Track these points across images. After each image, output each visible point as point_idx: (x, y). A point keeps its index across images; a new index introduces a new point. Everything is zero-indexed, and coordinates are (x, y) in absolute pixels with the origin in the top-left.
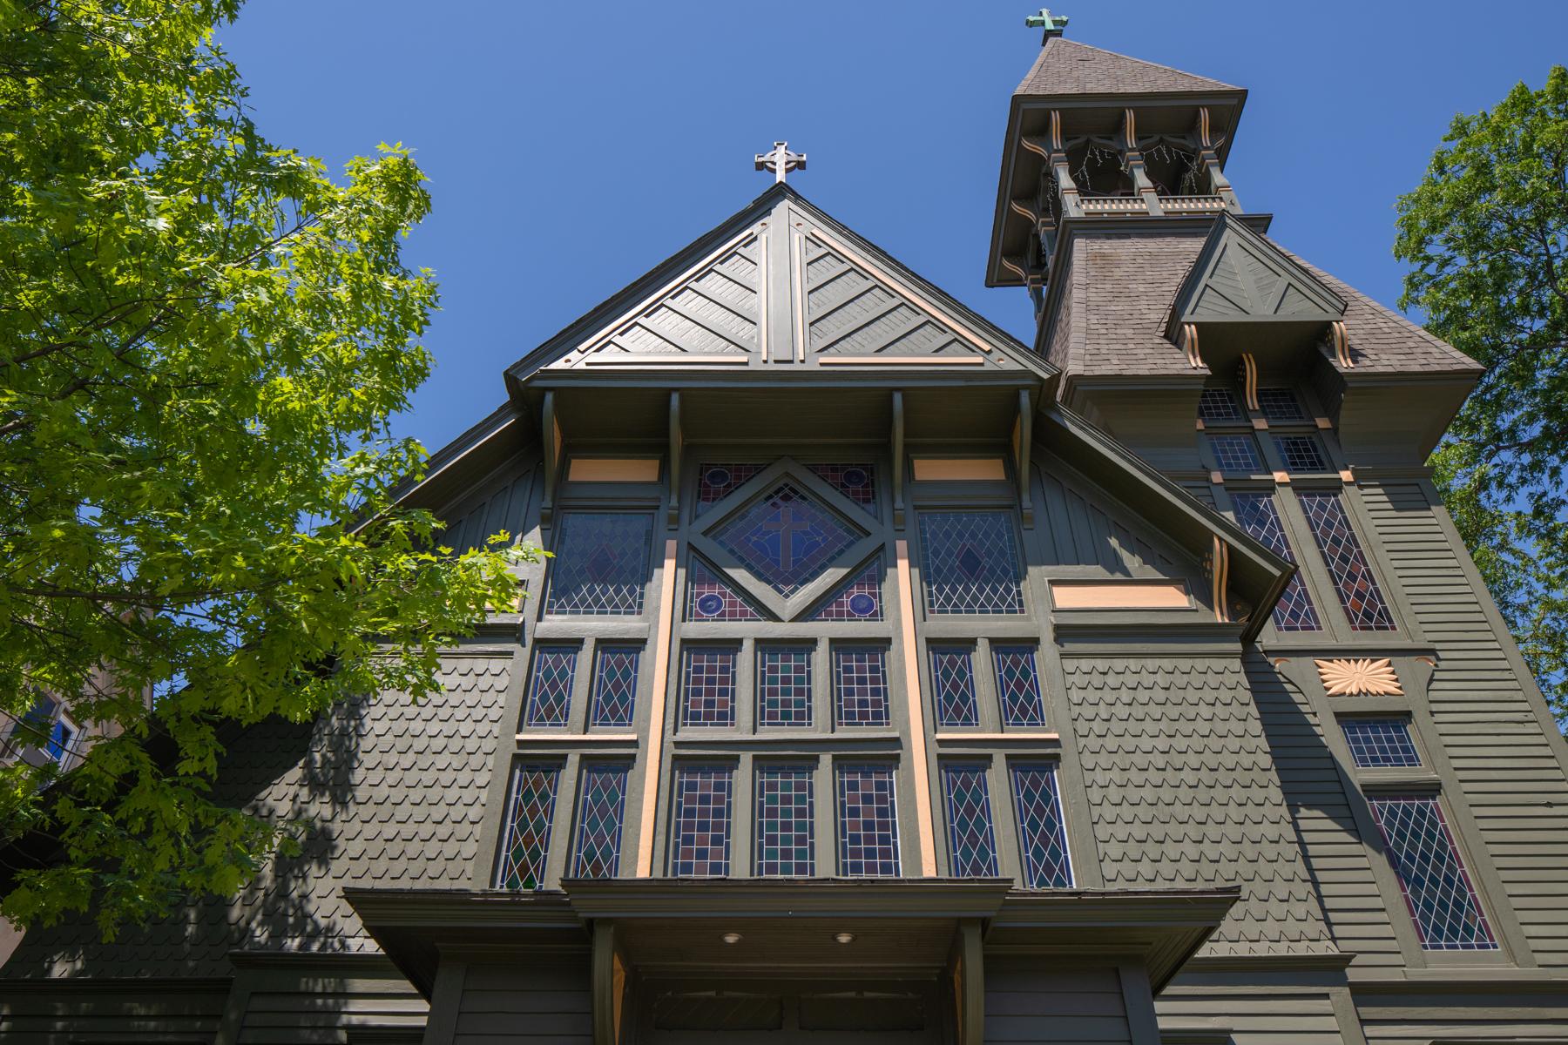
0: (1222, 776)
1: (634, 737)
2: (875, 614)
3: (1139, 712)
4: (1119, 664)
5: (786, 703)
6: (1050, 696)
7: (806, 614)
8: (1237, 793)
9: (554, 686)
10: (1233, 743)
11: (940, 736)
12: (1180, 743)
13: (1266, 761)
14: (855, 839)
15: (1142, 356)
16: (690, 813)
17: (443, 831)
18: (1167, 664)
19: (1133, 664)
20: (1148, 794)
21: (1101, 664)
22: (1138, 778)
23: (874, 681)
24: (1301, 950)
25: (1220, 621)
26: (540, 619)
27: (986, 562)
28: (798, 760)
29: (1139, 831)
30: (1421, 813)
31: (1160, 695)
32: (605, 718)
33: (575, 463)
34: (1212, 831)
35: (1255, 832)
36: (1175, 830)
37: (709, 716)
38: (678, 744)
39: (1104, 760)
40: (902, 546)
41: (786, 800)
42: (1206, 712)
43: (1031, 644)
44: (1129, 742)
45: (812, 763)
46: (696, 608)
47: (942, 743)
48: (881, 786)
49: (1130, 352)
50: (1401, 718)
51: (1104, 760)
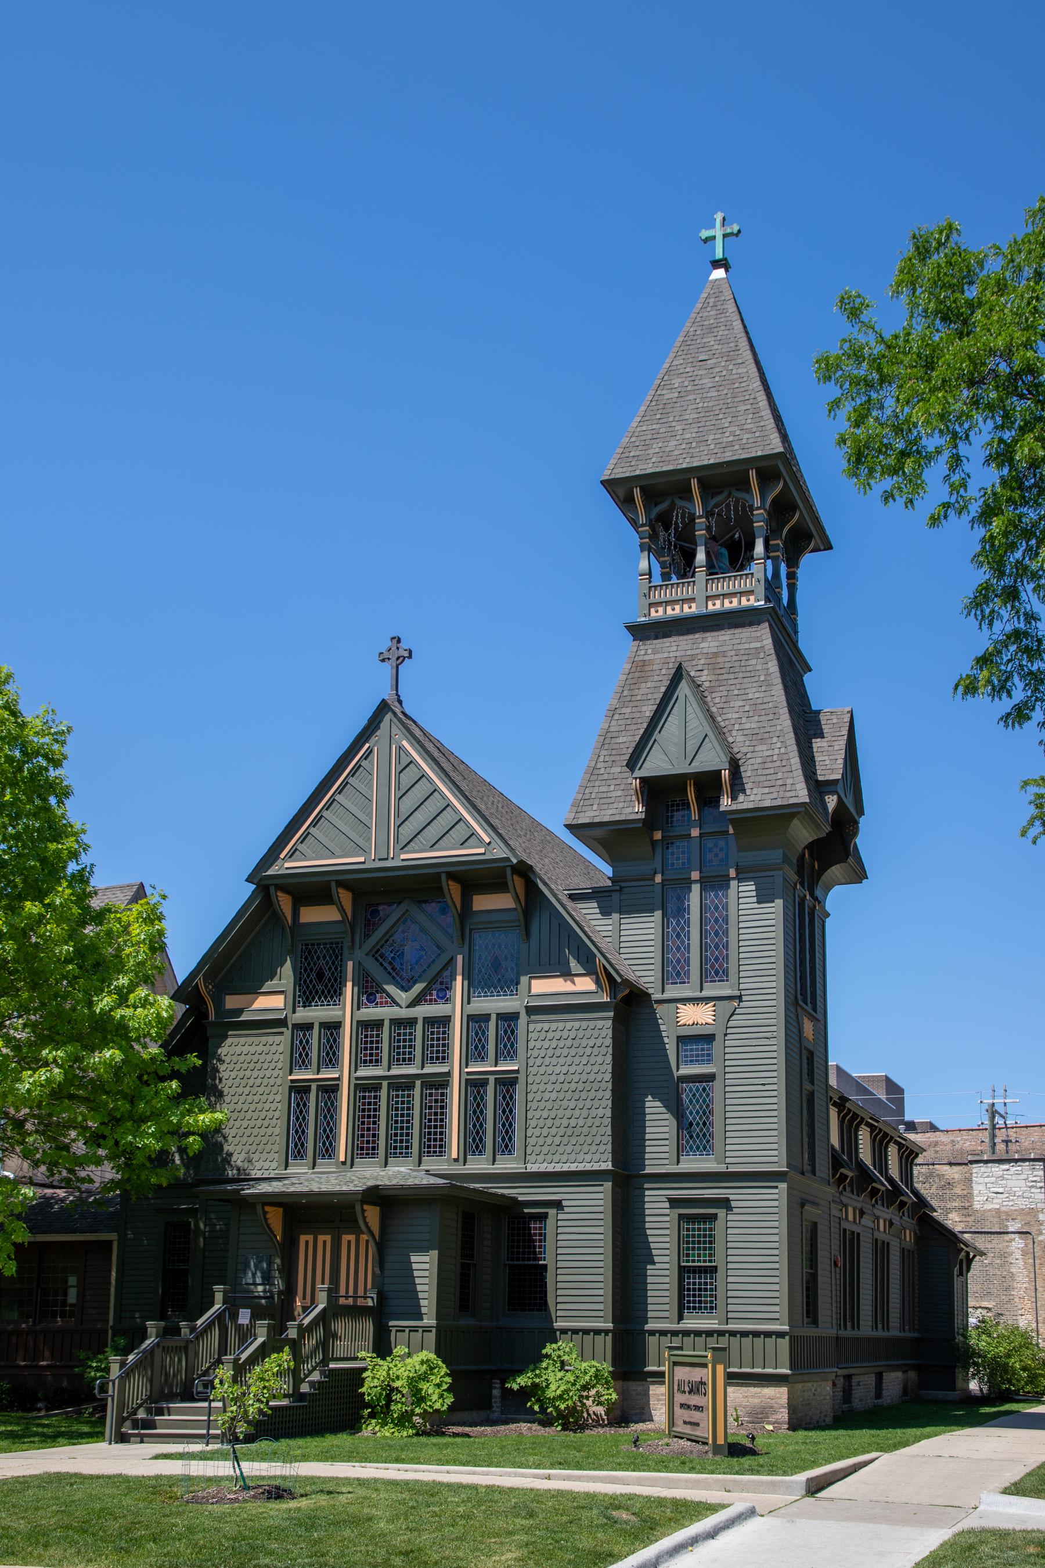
0: (588, 1086)
1: (337, 1076)
2: (447, 1000)
3: (558, 1052)
4: (554, 1026)
5: (404, 1053)
6: (521, 1046)
7: (412, 1004)
8: (592, 1094)
9: (304, 1048)
10: (596, 1068)
11: (467, 1070)
12: (572, 1069)
13: (608, 1077)
14: (430, 1120)
16: (364, 1110)
17: (266, 1123)
18: (577, 1024)
19: (561, 1025)
20: (553, 1096)
21: (546, 1026)
22: (550, 1087)
23: (444, 1039)
25: (605, 1000)
28: (402, 1085)
29: (545, 1114)
30: (704, 1089)
31: (569, 1043)
32: (327, 1065)
34: (577, 1113)
35: (593, 1112)
36: (560, 1113)
37: (371, 1061)
38: (357, 1079)
39: (537, 1079)
40: (460, 958)
42: (588, 1051)
43: (513, 1017)
44: (550, 1070)
45: (411, 1087)
46: (365, 1001)
47: (468, 1073)
48: (442, 1094)
49: (609, 795)
50: (709, 1038)
51: (537, 1079)
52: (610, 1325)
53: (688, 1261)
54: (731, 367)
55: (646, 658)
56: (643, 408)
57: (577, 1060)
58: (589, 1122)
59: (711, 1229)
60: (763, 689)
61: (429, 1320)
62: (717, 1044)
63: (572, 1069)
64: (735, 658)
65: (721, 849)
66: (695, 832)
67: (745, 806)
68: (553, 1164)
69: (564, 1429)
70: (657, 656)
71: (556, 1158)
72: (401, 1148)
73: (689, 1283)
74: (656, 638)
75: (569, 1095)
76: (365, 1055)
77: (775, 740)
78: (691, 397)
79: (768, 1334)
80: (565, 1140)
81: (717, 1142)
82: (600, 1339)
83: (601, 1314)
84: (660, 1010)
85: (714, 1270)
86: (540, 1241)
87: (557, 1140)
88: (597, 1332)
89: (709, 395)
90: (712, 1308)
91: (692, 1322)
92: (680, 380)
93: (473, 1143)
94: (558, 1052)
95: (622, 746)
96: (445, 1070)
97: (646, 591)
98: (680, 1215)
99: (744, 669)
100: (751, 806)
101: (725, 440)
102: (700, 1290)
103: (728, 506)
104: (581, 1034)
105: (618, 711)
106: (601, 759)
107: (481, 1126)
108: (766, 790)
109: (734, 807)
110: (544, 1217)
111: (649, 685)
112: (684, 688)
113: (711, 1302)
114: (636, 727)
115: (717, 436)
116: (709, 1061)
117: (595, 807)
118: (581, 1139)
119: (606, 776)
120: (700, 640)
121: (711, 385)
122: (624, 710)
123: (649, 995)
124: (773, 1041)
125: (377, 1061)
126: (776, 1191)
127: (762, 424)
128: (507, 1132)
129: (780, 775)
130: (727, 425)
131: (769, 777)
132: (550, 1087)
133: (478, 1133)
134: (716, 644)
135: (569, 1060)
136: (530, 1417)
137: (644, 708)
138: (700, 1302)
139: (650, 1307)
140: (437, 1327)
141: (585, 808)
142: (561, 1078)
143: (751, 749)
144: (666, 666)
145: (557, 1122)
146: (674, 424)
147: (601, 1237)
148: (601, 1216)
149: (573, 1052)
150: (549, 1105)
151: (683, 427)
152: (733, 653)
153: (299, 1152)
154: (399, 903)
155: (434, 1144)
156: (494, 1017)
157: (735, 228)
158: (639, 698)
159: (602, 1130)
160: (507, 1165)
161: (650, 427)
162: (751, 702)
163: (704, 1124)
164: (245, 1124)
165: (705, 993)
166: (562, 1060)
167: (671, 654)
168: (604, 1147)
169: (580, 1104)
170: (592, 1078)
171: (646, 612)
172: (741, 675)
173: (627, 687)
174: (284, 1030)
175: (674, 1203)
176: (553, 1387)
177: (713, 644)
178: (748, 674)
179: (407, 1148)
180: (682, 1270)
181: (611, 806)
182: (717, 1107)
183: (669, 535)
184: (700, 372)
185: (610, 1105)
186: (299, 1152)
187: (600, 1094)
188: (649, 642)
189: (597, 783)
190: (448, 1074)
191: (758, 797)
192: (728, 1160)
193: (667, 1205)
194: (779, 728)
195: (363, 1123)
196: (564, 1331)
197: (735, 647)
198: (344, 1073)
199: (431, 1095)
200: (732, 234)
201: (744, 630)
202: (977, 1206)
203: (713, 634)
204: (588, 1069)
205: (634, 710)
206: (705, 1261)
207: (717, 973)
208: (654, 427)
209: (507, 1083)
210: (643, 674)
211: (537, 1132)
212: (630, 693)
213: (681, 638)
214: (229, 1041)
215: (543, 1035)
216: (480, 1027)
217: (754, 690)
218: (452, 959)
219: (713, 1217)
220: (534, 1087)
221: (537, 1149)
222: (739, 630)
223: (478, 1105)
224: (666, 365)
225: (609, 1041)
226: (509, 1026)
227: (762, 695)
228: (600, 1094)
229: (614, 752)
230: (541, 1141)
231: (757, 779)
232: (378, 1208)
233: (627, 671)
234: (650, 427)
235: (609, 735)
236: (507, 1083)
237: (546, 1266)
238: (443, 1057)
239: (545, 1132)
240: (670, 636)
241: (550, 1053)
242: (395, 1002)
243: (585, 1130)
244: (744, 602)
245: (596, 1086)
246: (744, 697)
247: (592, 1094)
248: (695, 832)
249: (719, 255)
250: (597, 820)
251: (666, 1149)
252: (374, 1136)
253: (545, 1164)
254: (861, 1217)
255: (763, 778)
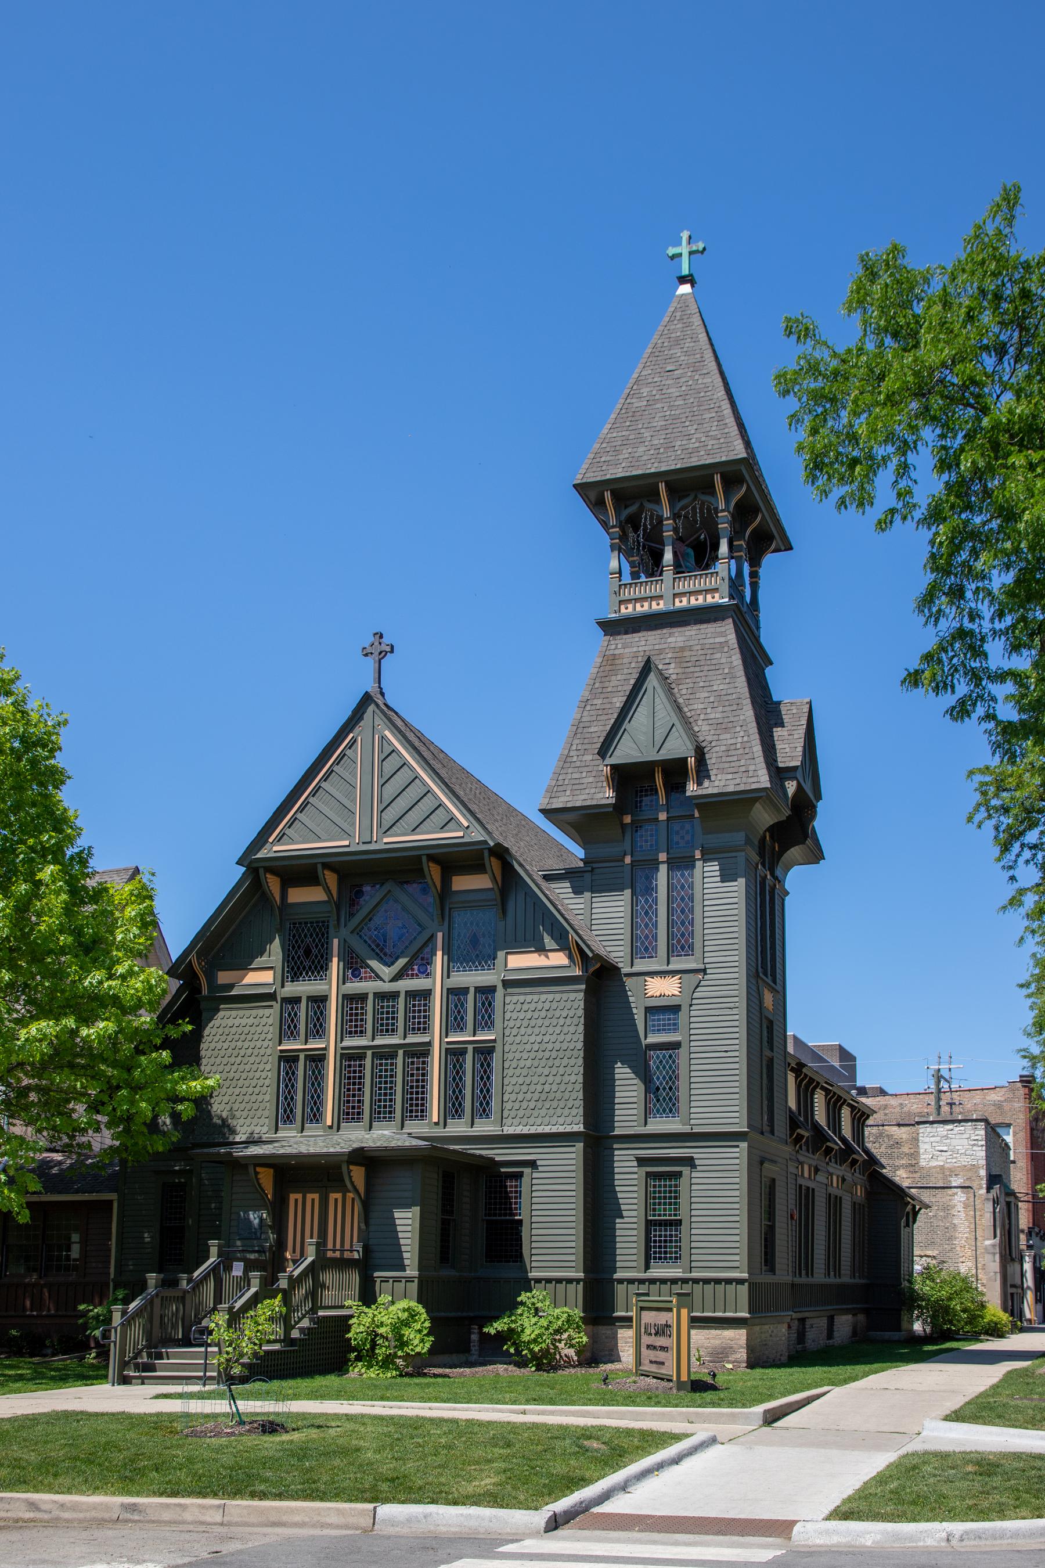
0: (561, 1054)
1: (324, 1046)
3: (533, 1023)
4: (529, 998)
5: (387, 1024)
6: (497, 1017)
8: (565, 1062)
9: (292, 1021)
10: (568, 1037)
12: (546, 1039)
14: (412, 1087)
15: (584, 786)
16: (349, 1078)
17: (257, 1090)
18: (550, 997)
19: (536, 998)
20: (529, 1063)
21: (521, 998)
23: (425, 1011)
24: (569, 1129)
26: (283, 986)
27: (482, 940)
28: (386, 1054)
29: (521, 1080)
30: (671, 1056)
31: (543, 1014)
33: (290, 890)
34: (550, 1079)
35: (566, 1078)
36: (535, 1079)
37: (356, 1032)
38: (343, 1048)
39: (514, 1048)
40: (440, 935)
41: (386, 1070)
42: (561, 1021)
43: (491, 990)
44: (525, 1039)
45: (394, 1056)
47: (448, 1043)
48: (424, 1063)
49: (582, 781)
50: (675, 1009)
51: (514, 1048)
52: (581, 1275)
53: (654, 1215)
54: (696, 377)
55: (617, 652)
56: (613, 416)
57: (550, 1030)
58: (562, 1087)
59: (676, 1186)
60: (727, 681)
61: (412, 1272)
62: (683, 1015)
63: (546, 1039)
64: (701, 652)
65: (687, 832)
66: (663, 816)
67: (710, 791)
68: (528, 1127)
69: (538, 1370)
70: (626, 650)
71: (531, 1121)
72: (385, 1112)
73: (655, 1236)
74: (626, 633)
75: (543, 1063)
76: (351, 1027)
77: (738, 729)
78: (659, 406)
79: (729, 1281)
80: (539, 1104)
81: (682, 1105)
82: (571, 1287)
83: (573, 1264)
84: (629, 982)
85: (679, 1223)
86: (516, 1198)
87: (532, 1105)
88: (569, 1281)
89: (677, 403)
90: (676, 1258)
91: (658, 1271)
92: (648, 389)
93: (453, 1108)
94: (533, 1023)
95: (594, 735)
96: (427, 1040)
97: (617, 589)
98: (647, 1173)
99: (709, 662)
100: (715, 791)
101: (691, 446)
102: (665, 1241)
103: (694, 509)
104: (554, 1005)
105: (590, 702)
106: (574, 747)
107: (460, 1091)
108: (730, 776)
109: (700, 792)
110: (519, 1176)
111: (619, 677)
112: (652, 680)
113: (676, 1252)
114: (606, 717)
115: (684, 442)
116: (676, 1030)
117: (568, 793)
118: (555, 1104)
119: (578, 764)
120: (667, 635)
121: (678, 394)
122: (595, 702)
123: (619, 969)
124: (735, 1011)
125: (361, 1032)
126: (737, 1150)
127: (726, 431)
128: (485, 1097)
129: (742, 762)
130: (693, 432)
131: (733, 764)
132: (525, 1055)
133: (457, 1098)
134: (683, 639)
135: (543, 1030)
136: (506, 1359)
137: (615, 700)
138: (665, 1253)
139: (618, 1258)
140: (420, 1277)
141: (558, 794)
142: (536, 1047)
143: (716, 738)
144: (635, 660)
145: (532, 1088)
146: (642, 431)
147: (574, 1193)
148: (573, 1174)
149: (547, 1022)
150: (525, 1072)
151: (652, 433)
152: (699, 647)
153: (288, 1117)
154: (382, 884)
155: (416, 1108)
156: (472, 990)
157: (701, 246)
158: (609, 690)
159: (574, 1095)
160: (485, 1127)
161: (620, 434)
162: (716, 693)
163: (671, 1088)
164: (237, 1091)
165: (671, 967)
166: (537, 1030)
167: (641, 649)
168: (576, 1111)
169: (554, 1071)
170: (564, 1046)
171: (617, 608)
172: (706, 668)
173: (598, 680)
174: (273, 1003)
175: (642, 1161)
176: (528, 1331)
177: (679, 639)
178: (713, 667)
179: (390, 1112)
180: (649, 1224)
181: (583, 792)
182: (683, 1072)
183: (638, 536)
184: (668, 382)
185: (582, 1072)
186: (288, 1117)
187: (572, 1062)
188: (619, 637)
189: (570, 771)
190: (429, 1044)
191: (722, 783)
192: (692, 1122)
193: (635, 1164)
194: (742, 717)
195: (349, 1090)
196: (538, 1281)
197: (701, 642)
198: (331, 1043)
199: (413, 1063)
200: (697, 252)
201: (709, 625)
202: (923, 1163)
203: (680, 629)
204: (561, 1038)
205: (605, 701)
206: (670, 1215)
207: (683, 948)
208: (624, 433)
209: (485, 1051)
210: (613, 667)
211: (513, 1097)
212: (601, 685)
213: (650, 633)
214: (221, 1014)
215: (519, 1006)
216: (459, 1000)
217: (719, 682)
218: (432, 936)
219: (679, 1174)
220: (510, 1056)
221: (513, 1113)
222: (705, 626)
223: (458, 1073)
224: (635, 375)
225: (581, 1012)
226: (487, 998)
227: (726, 686)
228: (572, 1062)
229: (586, 741)
230: (517, 1105)
231: (721, 766)
232: (363, 1169)
233: (598, 665)
234: (620, 434)
235: (581, 725)
236: (485, 1051)
237: (521, 1221)
238: (424, 1027)
239: (520, 1097)
240: (639, 632)
241: (525, 1023)
242: (378, 976)
243: (559, 1095)
244: (709, 599)
245: (568, 1053)
246: (709, 689)
247: (565, 1062)
248: (663, 816)
249: (685, 271)
250: (569, 805)
251: (635, 1112)
252: (359, 1101)
253: (521, 1127)
254: (816, 1173)
255: (727, 765)
